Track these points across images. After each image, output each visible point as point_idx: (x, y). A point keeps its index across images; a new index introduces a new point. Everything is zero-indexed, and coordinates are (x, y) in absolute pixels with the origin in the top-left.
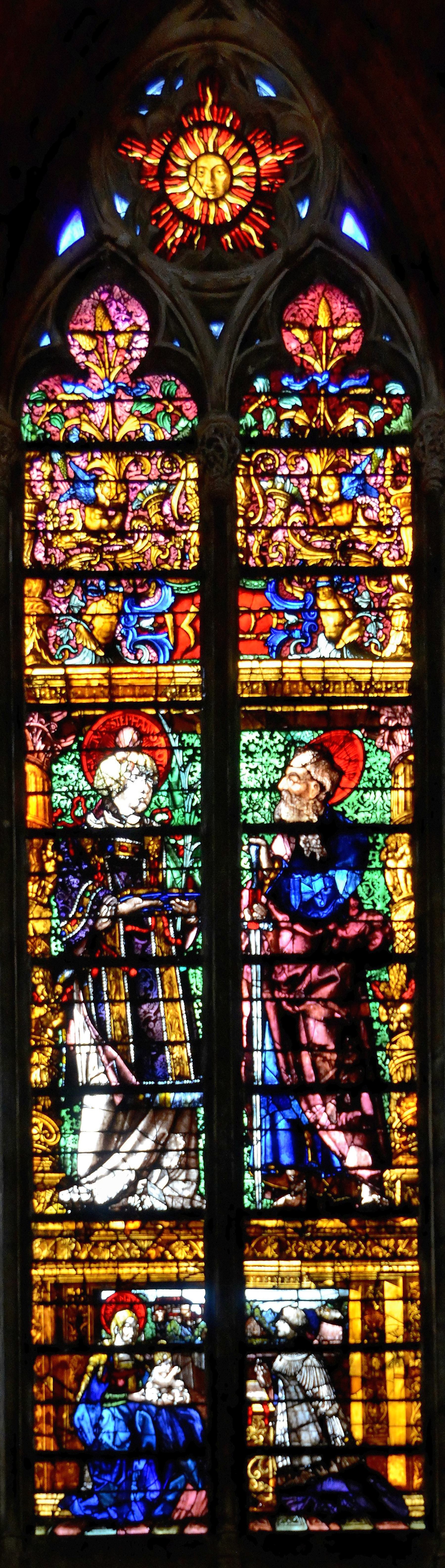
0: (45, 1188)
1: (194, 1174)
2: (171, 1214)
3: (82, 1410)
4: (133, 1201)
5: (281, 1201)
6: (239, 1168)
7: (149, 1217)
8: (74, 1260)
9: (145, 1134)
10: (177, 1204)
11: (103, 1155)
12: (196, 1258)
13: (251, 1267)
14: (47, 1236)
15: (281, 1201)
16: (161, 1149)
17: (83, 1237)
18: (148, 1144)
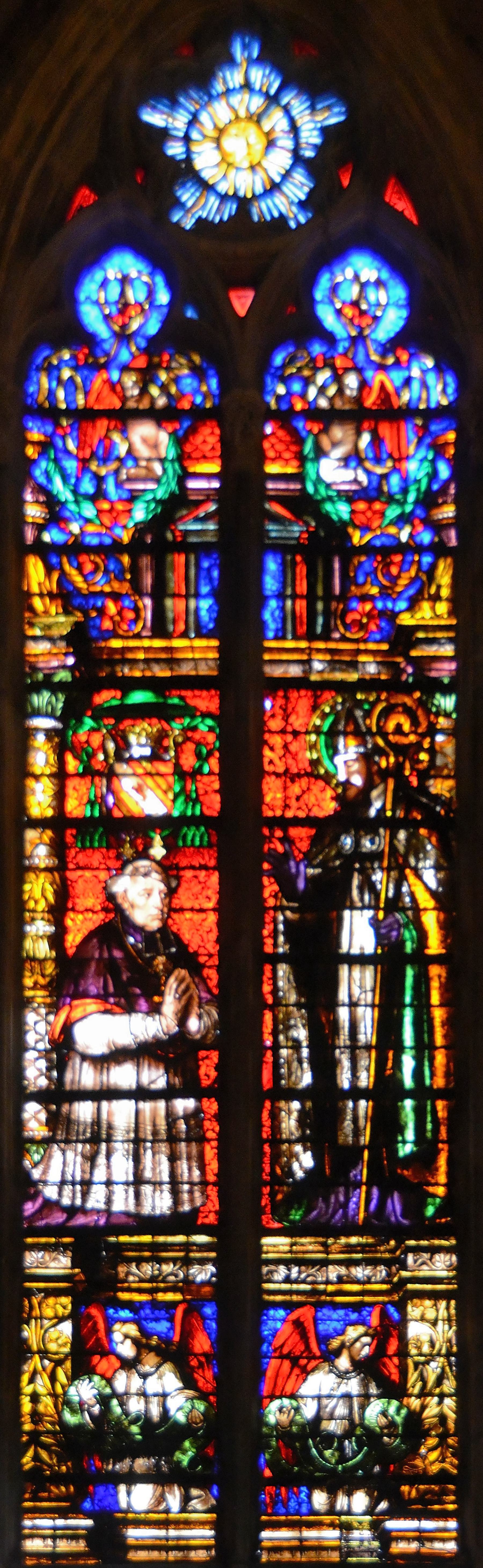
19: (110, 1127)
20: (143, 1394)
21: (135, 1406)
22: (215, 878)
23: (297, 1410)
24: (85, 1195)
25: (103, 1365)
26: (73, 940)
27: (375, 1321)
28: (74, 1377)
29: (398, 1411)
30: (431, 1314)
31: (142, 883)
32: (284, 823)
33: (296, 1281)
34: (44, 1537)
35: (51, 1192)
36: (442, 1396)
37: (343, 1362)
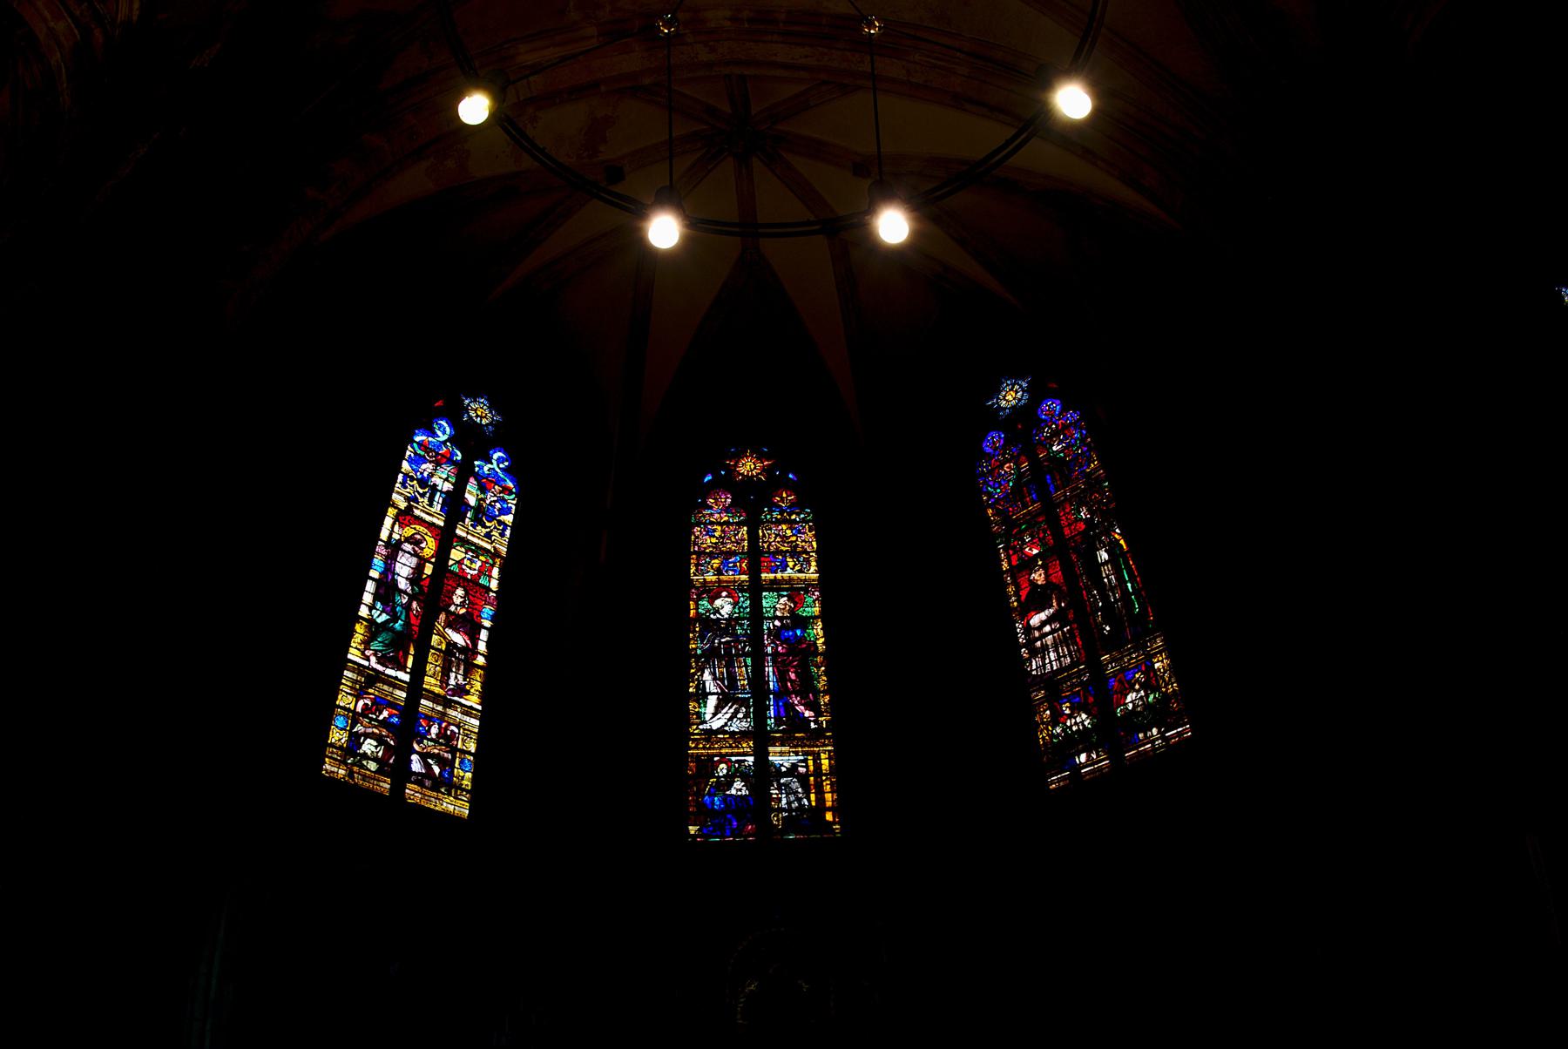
0: (694, 724)
1: (749, 720)
2: (741, 732)
3: (707, 797)
4: (727, 728)
5: (781, 728)
6: (766, 718)
7: (733, 734)
8: (704, 748)
9: (730, 707)
10: (743, 729)
11: (714, 715)
12: (750, 747)
13: (771, 749)
14: (694, 740)
15: (781, 728)
16: (737, 712)
17: (708, 740)
18: (732, 710)
19: (1047, 645)
20: (1076, 723)
21: (1074, 728)
22: (1058, 562)
23: (1127, 709)
24: (1045, 669)
25: (1062, 720)
26: (1023, 598)
27: (1143, 668)
28: (1054, 728)
29: (1159, 695)
30: (1160, 659)
31: (1038, 573)
32: (1073, 537)
33: (1116, 667)
34: (1055, 783)
35: (1034, 673)
36: (1172, 684)
37: (1137, 687)
